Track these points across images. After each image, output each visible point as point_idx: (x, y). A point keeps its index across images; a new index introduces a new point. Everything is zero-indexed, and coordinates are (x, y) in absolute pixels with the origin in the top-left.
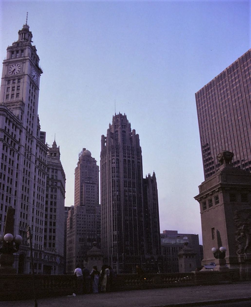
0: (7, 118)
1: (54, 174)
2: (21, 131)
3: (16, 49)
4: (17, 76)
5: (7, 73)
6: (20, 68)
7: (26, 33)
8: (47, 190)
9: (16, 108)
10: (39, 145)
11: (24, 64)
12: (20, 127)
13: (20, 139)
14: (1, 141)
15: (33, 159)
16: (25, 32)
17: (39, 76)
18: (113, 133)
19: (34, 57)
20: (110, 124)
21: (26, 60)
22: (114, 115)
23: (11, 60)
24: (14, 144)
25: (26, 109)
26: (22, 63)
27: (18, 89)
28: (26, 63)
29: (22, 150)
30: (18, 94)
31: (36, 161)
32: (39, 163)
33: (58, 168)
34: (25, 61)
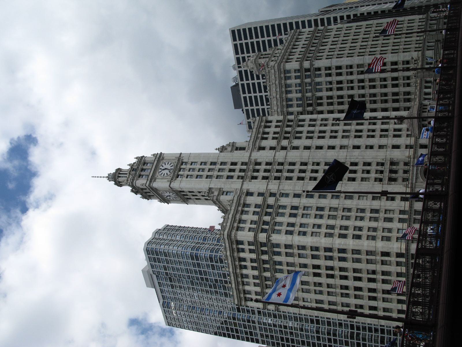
0: (238, 229)
1: (293, 74)
2: (249, 194)
7: (117, 178)
8: (321, 112)
9: (219, 202)
10: (257, 145)
12: (242, 199)
13: (260, 194)
14: (271, 238)
15: (280, 156)
17: (163, 158)
19: (142, 170)
24: (269, 206)
25: (215, 184)
29: (273, 186)
32: (285, 138)
33: (282, 70)
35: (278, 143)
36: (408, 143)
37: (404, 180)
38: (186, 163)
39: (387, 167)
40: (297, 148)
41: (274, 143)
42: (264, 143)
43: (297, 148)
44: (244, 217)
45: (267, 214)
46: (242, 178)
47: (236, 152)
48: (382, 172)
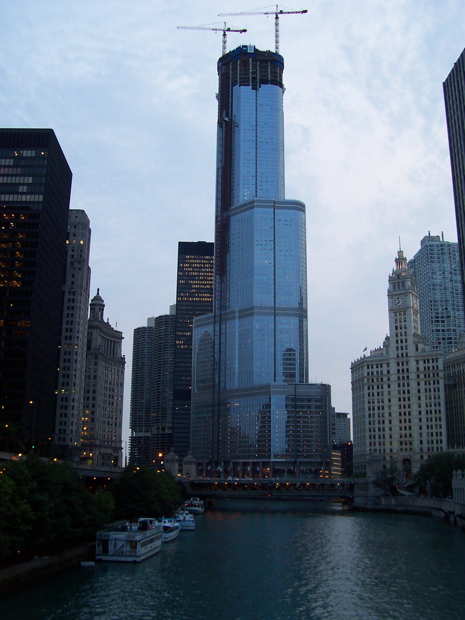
2: (388, 365)
15: (413, 376)
29: (393, 378)
31: (418, 376)
35: (421, 372)
36: (424, 448)
37: (402, 450)
38: (405, 314)
39: (408, 439)
40: (419, 384)
41: (421, 369)
42: (421, 364)
43: (419, 384)
44: (375, 367)
45: (378, 379)
46: (398, 356)
47: (415, 346)
48: (406, 436)
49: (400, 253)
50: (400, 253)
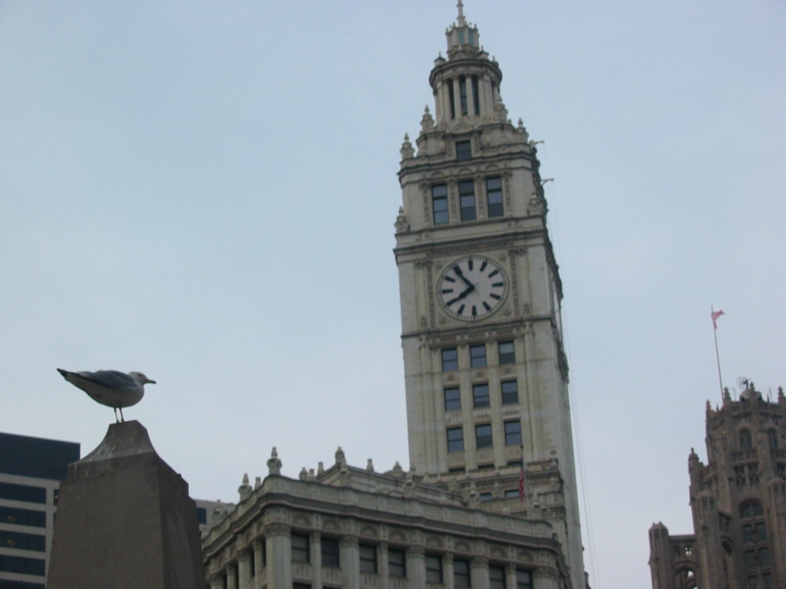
3: (455, 171)
4: (495, 325)
5: (432, 306)
6: (498, 278)
11: (521, 260)
16: (474, 70)
18: (728, 518)
20: (693, 458)
21: (527, 235)
22: (717, 404)
23: (441, 236)
26: (505, 252)
27: (510, 398)
28: (530, 250)
30: (512, 426)
34: (519, 243)
49: (463, 37)
50: (463, 37)
